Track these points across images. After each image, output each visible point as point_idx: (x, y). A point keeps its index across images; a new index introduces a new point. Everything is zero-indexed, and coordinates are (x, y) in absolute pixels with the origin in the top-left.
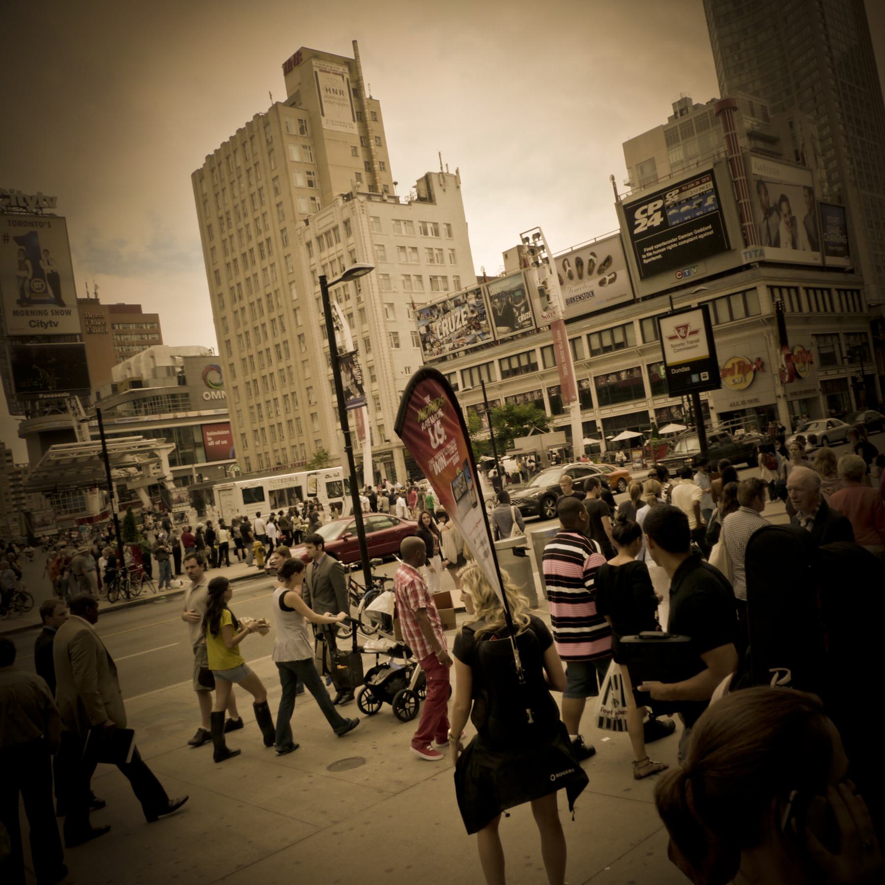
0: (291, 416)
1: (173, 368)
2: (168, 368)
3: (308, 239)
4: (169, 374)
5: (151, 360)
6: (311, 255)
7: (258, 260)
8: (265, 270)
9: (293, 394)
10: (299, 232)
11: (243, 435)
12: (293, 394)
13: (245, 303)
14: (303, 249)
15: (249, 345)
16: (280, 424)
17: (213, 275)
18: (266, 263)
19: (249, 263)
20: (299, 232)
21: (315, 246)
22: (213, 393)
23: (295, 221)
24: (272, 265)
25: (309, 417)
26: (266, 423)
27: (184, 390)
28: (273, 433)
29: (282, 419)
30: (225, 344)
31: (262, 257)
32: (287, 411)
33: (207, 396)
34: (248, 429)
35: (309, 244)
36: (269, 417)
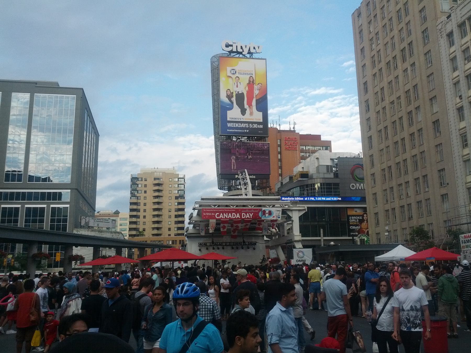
0: (421, 197)
1: (331, 167)
2: (327, 166)
3: (448, 30)
4: (328, 171)
5: (316, 160)
6: (452, 43)
7: (399, 64)
8: (406, 70)
9: (425, 176)
10: (440, 27)
11: (376, 214)
12: (425, 176)
13: (387, 102)
14: (443, 42)
15: (387, 138)
16: (409, 205)
17: (362, 86)
18: (407, 65)
19: (392, 67)
20: (440, 27)
21: (456, 35)
22: (358, 185)
23: (436, 19)
24: (413, 65)
25: (439, 198)
26: (397, 204)
27: (337, 181)
28: (402, 212)
29: (412, 200)
30: (368, 141)
31: (404, 60)
32: (417, 193)
33: (353, 186)
34: (380, 208)
35: (450, 35)
36: (400, 199)
